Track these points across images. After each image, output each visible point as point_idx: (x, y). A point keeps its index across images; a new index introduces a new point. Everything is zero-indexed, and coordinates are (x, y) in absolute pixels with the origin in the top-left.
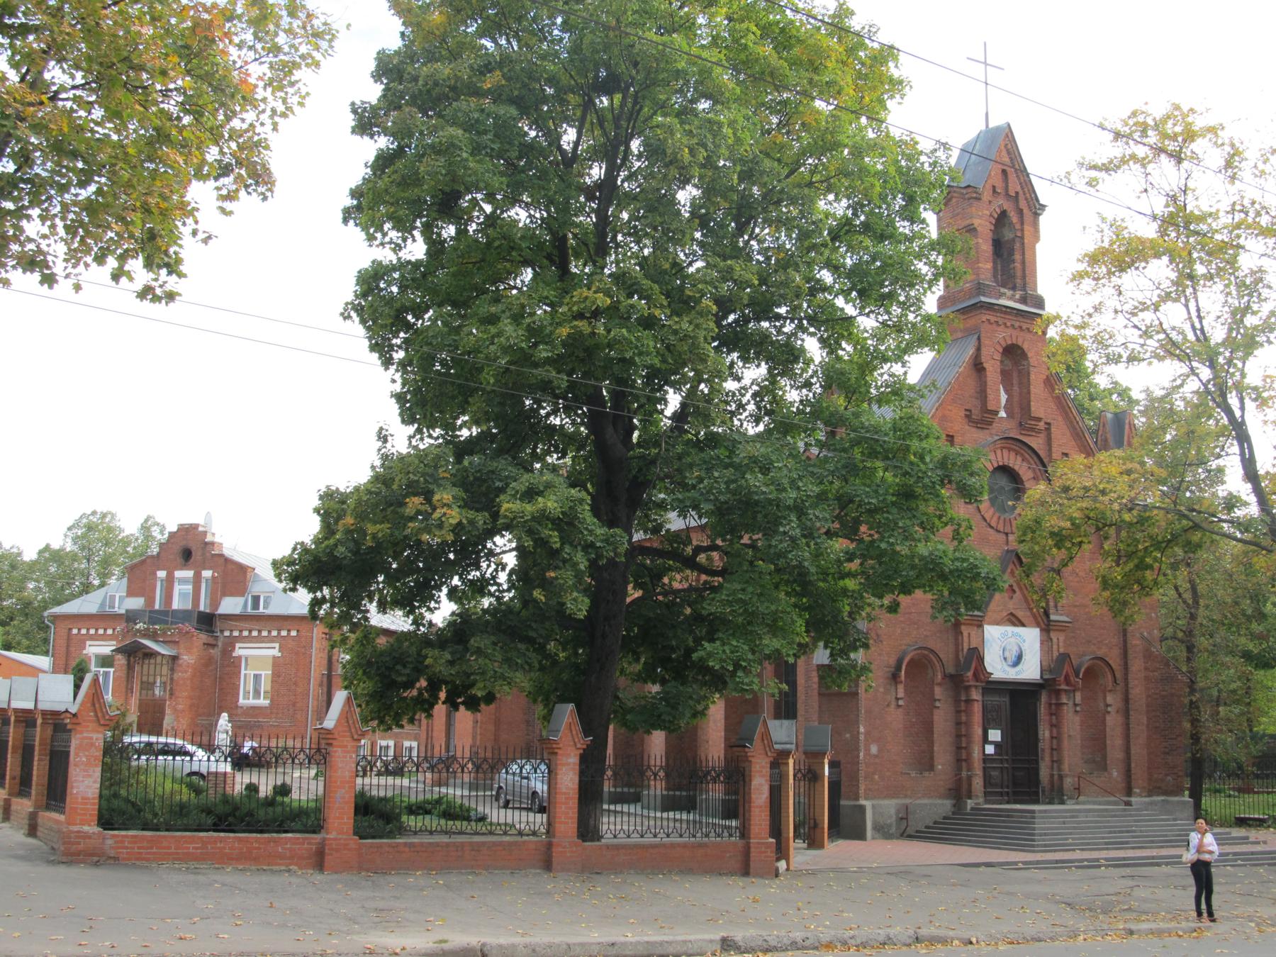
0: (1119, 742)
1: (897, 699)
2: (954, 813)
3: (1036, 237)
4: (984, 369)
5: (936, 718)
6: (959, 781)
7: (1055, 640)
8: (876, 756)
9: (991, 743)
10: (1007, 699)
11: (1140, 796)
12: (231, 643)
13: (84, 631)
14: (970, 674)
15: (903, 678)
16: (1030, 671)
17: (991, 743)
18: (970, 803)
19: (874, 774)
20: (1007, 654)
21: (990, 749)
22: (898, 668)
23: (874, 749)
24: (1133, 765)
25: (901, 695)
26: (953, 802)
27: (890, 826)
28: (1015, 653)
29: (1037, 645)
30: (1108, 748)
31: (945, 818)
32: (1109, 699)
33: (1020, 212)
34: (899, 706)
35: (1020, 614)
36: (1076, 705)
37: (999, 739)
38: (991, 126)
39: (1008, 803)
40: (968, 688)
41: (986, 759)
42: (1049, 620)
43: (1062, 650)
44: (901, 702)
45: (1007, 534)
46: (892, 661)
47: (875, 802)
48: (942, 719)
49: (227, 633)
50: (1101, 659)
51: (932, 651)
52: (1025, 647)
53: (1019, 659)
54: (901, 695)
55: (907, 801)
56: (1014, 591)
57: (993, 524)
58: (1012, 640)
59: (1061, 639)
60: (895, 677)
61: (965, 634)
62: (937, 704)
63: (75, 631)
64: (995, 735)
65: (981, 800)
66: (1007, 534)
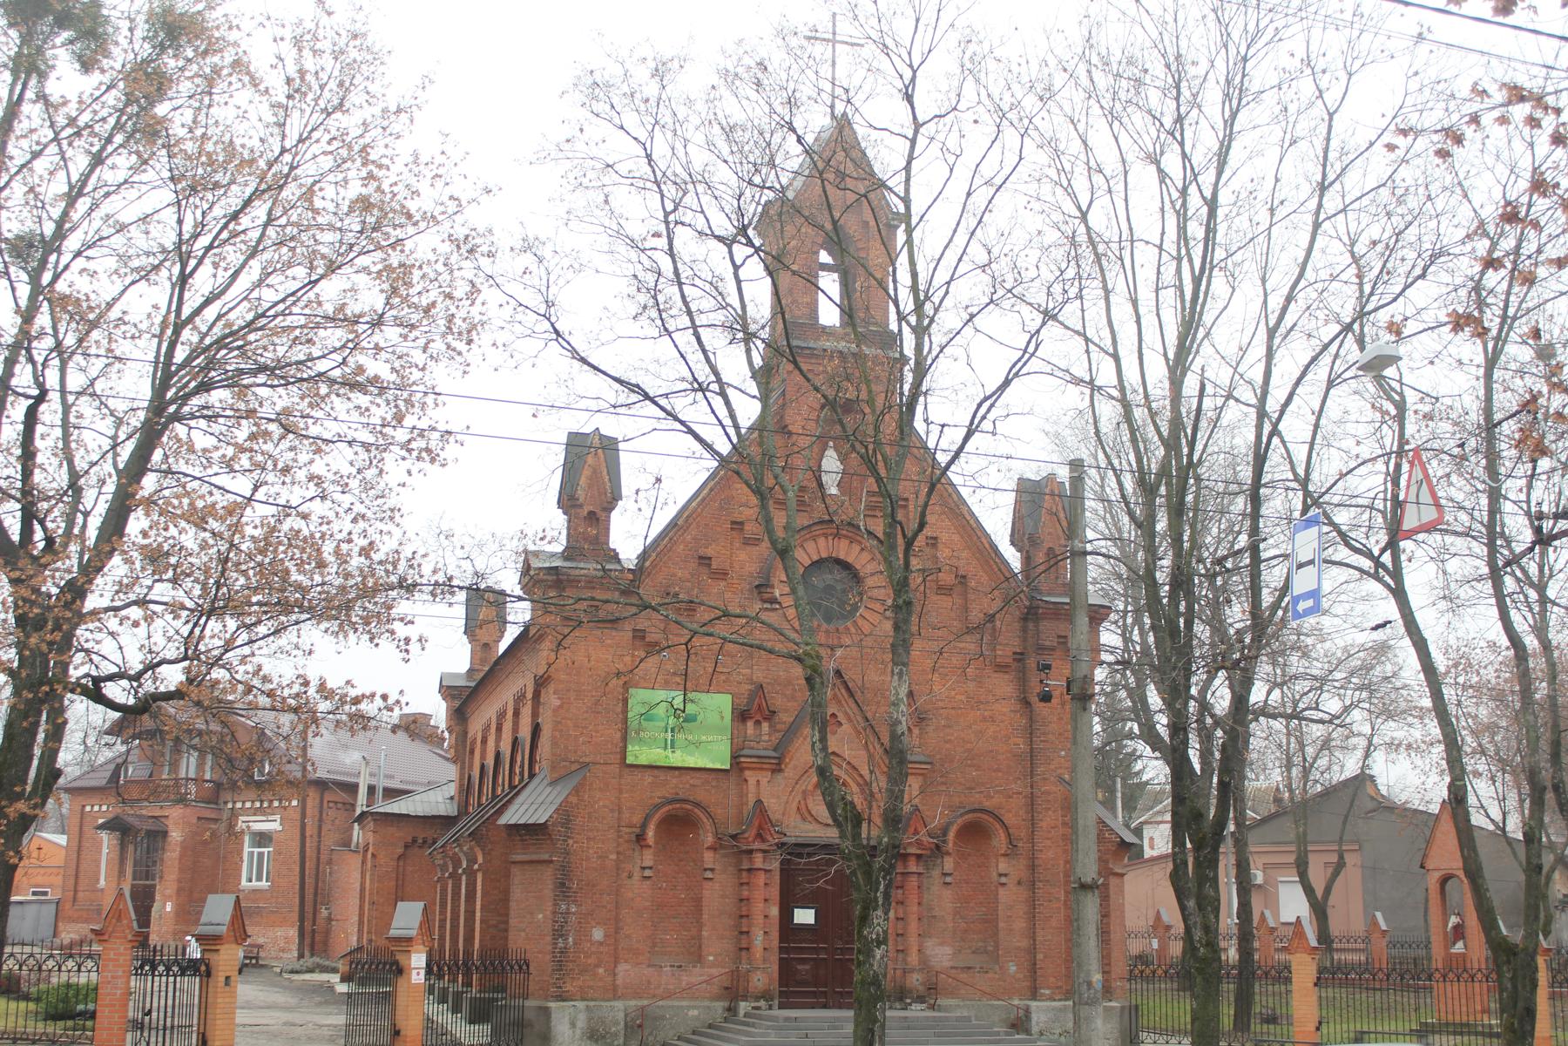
0: (1020, 924)
1: (643, 868)
2: (726, 1020)
5: (706, 893)
6: (736, 975)
8: (601, 944)
12: (234, 814)
13: (96, 808)
19: (598, 966)
22: (644, 826)
23: (598, 934)
24: (1040, 956)
26: (726, 1004)
27: (616, 1034)
30: (1001, 935)
31: (710, 1026)
37: (812, 921)
44: (647, 873)
46: (637, 819)
47: (592, 1003)
49: (230, 805)
51: (697, 805)
55: (645, 1002)
56: (840, 724)
61: (752, 781)
62: (709, 875)
63: (88, 808)
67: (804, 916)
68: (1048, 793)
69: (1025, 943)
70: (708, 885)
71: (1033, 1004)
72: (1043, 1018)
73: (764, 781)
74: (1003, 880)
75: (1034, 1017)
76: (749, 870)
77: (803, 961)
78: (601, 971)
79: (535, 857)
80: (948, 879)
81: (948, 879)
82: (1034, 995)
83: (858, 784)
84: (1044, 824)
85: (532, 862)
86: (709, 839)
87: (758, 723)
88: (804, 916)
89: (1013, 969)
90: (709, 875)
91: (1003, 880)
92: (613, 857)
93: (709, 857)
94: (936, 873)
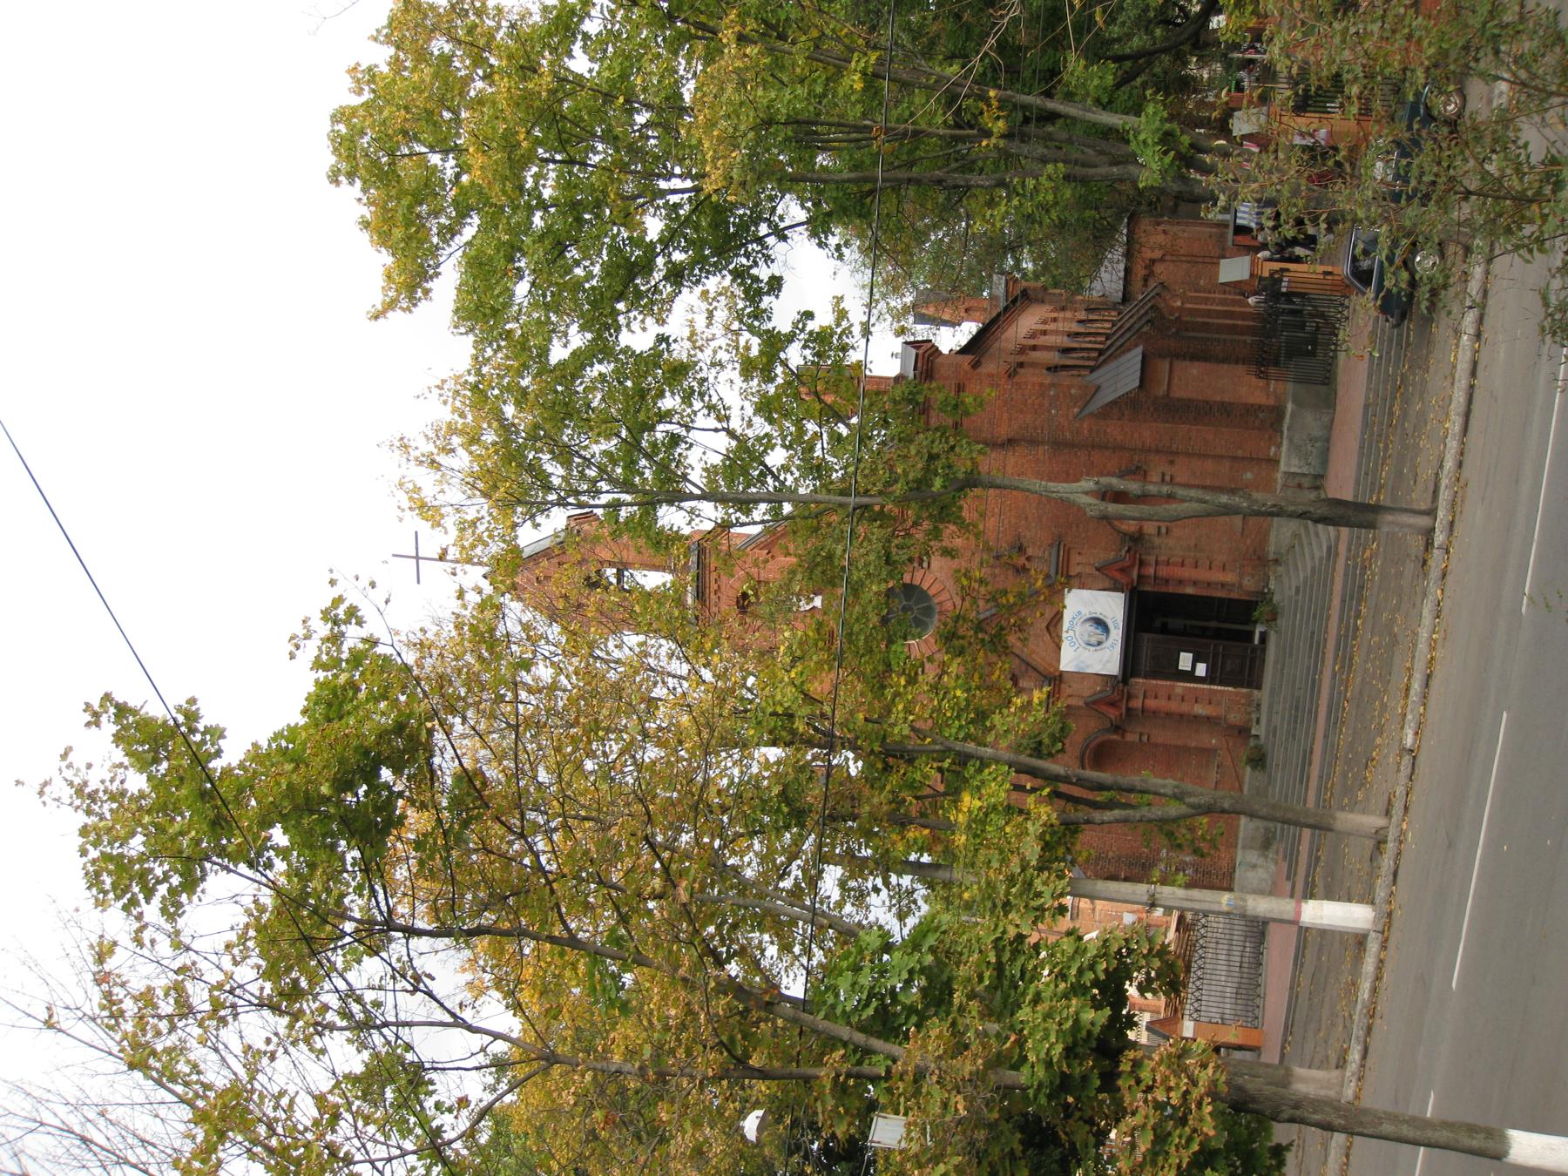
0: (1210, 465)
9: (1194, 667)
10: (1146, 636)
11: (1279, 446)
16: (1112, 606)
17: (1194, 667)
20: (1094, 640)
21: (1201, 670)
28: (1090, 628)
29: (1085, 593)
35: (1049, 615)
37: (1191, 655)
40: (1128, 710)
41: (1210, 678)
48: (1161, 735)
52: (1086, 614)
53: (1099, 623)
58: (1077, 629)
59: (1079, 559)
62: (1145, 738)
64: (1185, 661)
68: (1090, 430)
69: (1227, 464)
70: (1153, 739)
71: (1283, 467)
72: (1295, 461)
73: (1069, 691)
74: (1167, 478)
75: (1293, 470)
77: (1223, 663)
82: (1275, 462)
84: (1119, 438)
89: (1249, 475)
90: (1145, 738)
91: (1167, 478)
94: (1157, 541)
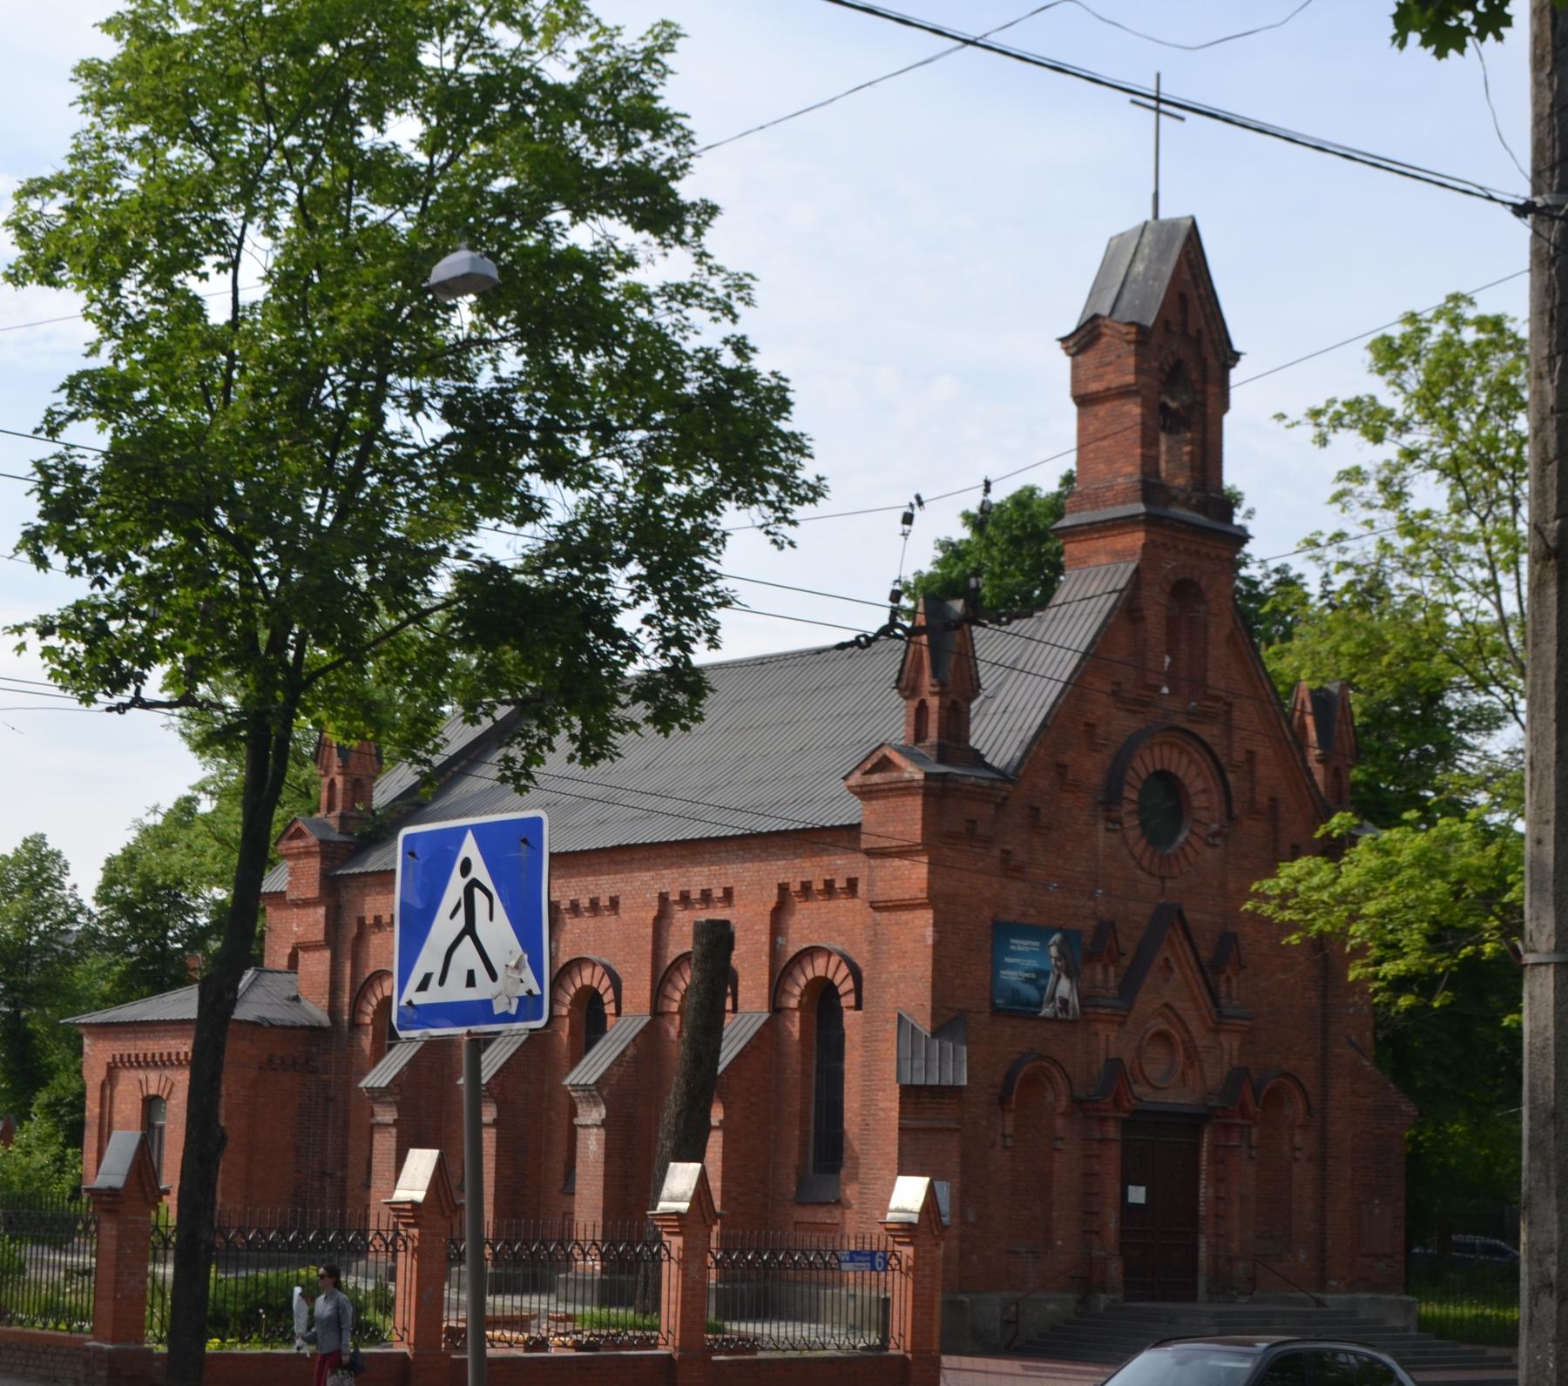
1: (1004, 1136)
3: (1225, 406)
4: (1143, 619)
7: (1226, 1045)
11: (1337, 1291)
14: (1109, 1100)
15: (1013, 1106)
18: (1103, 1300)
25: (1009, 1130)
32: (1298, 1139)
33: (1203, 363)
34: (1005, 1147)
36: (1250, 1147)
37: (1142, 1201)
38: (1163, 216)
39: (1153, 1299)
40: (1103, 1120)
42: (1220, 1014)
43: (1235, 1062)
44: (1009, 1142)
45: (1163, 879)
50: (1288, 1075)
51: (1056, 1063)
54: (1009, 1130)
56: (1171, 970)
57: (1145, 863)
59: (1236, 1045)
60: (1003, 1101)
61: (1102, 1036)
62: (1060, 1145)
65: (1119, 1296)
66: (1163, 879)
67: (1137, 1195)
74: (1298, 1154)
76: (1100, 1141)
78: (974, 1257)
79: (936, 1124)
80: (1254, 1153)
81: (1254, 1153)
83: (1183, 1042)
85: (931, 1130)
86: (1064, 1102)
87: (1105, 967)
88: (1137, 1195)
91: (1298, 1154)
92: (984, 1123)
93: (1060, 1122)
